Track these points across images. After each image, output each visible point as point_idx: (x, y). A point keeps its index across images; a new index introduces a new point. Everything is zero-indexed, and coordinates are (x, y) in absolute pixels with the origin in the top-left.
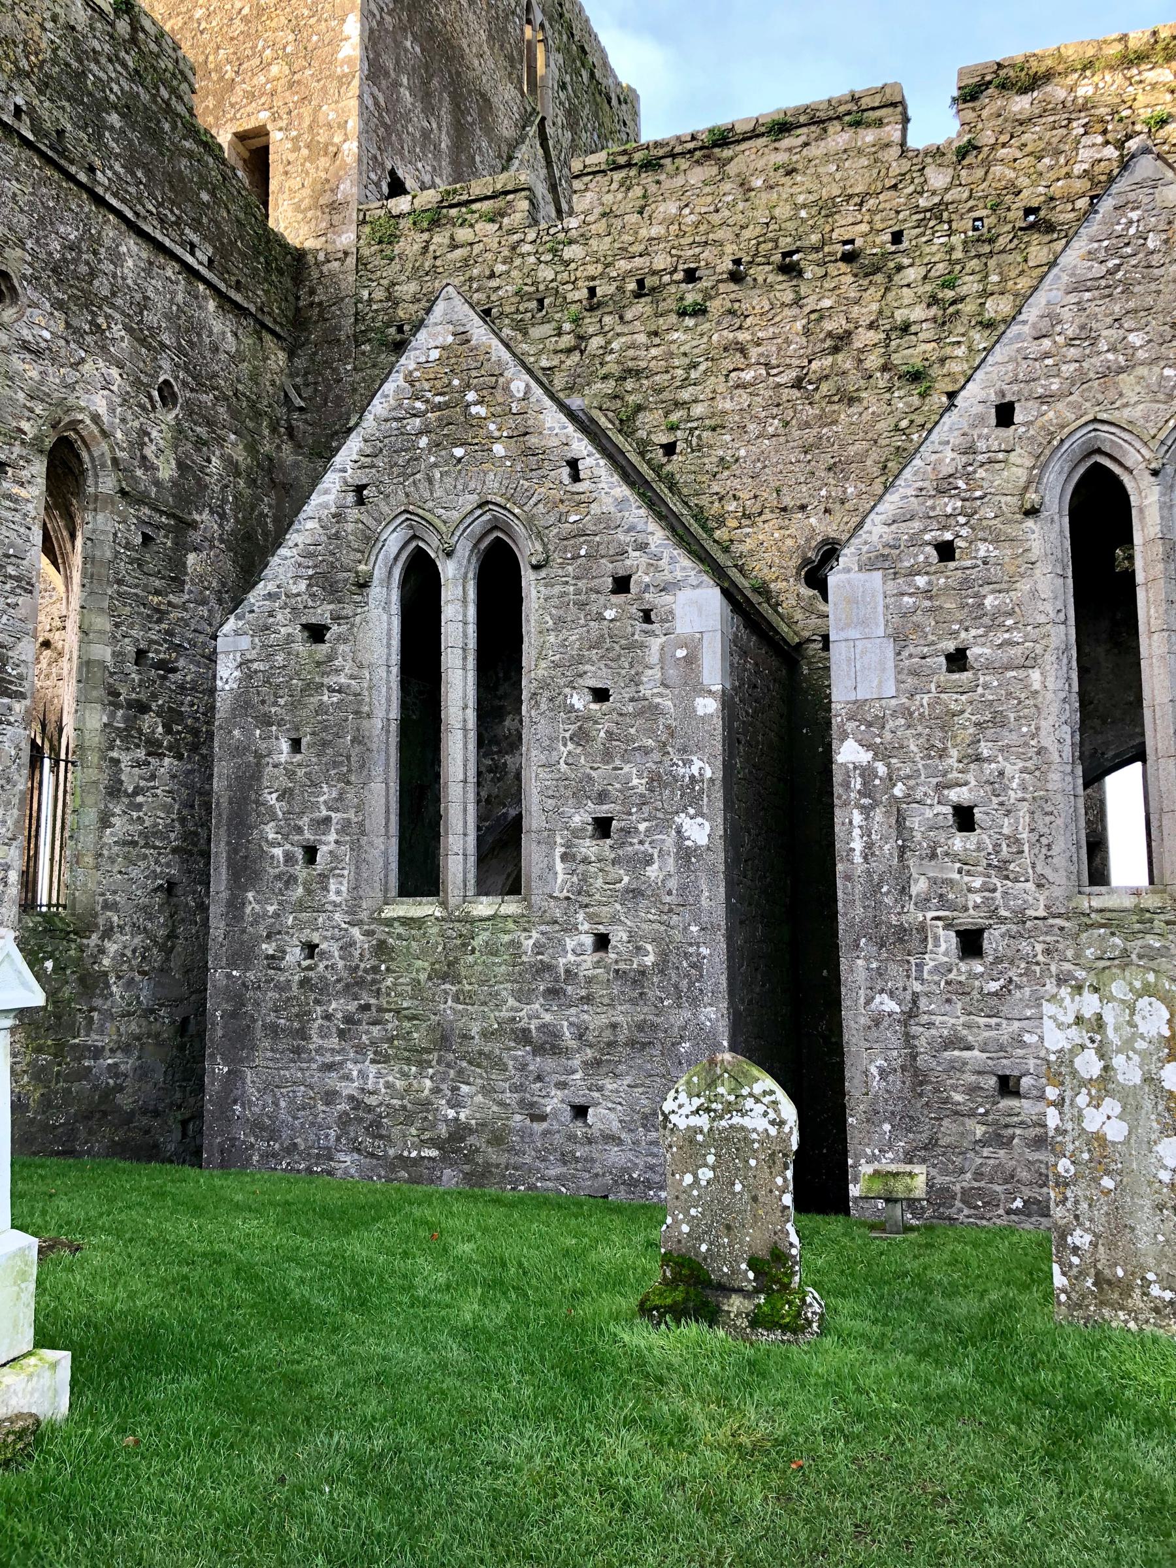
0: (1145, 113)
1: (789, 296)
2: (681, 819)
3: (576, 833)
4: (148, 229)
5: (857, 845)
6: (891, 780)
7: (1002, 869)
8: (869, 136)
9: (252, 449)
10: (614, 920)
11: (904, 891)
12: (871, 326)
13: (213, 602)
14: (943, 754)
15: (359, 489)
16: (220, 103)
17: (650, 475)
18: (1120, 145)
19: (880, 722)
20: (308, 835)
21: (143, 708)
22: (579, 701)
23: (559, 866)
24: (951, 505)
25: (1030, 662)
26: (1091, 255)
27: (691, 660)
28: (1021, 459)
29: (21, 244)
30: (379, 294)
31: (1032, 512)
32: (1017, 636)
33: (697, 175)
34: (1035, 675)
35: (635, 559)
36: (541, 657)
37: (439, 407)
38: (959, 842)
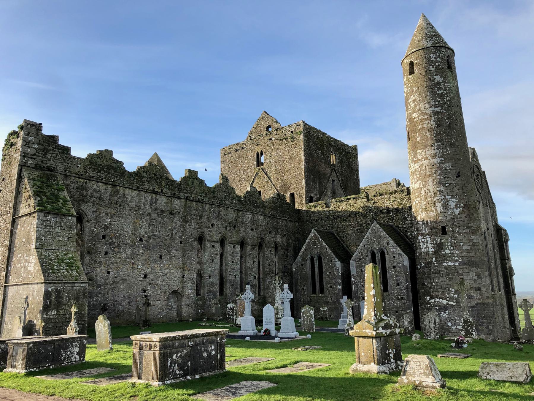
0: (392, 200)
1: (355, 219)
3: (329, 287)
6: (356, 282)
8: (363, 200)
9: (295, 237)
10: (332, 296)
11: (358, 293)
12: (364, 223)
13: (291, 258)
14: (361, 280)
15: (306, 250)
16: (288, 189)
17: (341, 241)
19: (355, 276)
20: (303, 287)
21: (285, 272)
24: (360, 255)
27: (338, 269)
28: (366, 251)
30: (309, 216)
31: (367, 256)
33: (345, 203)
36: (324, 268)
37: (313, 241)
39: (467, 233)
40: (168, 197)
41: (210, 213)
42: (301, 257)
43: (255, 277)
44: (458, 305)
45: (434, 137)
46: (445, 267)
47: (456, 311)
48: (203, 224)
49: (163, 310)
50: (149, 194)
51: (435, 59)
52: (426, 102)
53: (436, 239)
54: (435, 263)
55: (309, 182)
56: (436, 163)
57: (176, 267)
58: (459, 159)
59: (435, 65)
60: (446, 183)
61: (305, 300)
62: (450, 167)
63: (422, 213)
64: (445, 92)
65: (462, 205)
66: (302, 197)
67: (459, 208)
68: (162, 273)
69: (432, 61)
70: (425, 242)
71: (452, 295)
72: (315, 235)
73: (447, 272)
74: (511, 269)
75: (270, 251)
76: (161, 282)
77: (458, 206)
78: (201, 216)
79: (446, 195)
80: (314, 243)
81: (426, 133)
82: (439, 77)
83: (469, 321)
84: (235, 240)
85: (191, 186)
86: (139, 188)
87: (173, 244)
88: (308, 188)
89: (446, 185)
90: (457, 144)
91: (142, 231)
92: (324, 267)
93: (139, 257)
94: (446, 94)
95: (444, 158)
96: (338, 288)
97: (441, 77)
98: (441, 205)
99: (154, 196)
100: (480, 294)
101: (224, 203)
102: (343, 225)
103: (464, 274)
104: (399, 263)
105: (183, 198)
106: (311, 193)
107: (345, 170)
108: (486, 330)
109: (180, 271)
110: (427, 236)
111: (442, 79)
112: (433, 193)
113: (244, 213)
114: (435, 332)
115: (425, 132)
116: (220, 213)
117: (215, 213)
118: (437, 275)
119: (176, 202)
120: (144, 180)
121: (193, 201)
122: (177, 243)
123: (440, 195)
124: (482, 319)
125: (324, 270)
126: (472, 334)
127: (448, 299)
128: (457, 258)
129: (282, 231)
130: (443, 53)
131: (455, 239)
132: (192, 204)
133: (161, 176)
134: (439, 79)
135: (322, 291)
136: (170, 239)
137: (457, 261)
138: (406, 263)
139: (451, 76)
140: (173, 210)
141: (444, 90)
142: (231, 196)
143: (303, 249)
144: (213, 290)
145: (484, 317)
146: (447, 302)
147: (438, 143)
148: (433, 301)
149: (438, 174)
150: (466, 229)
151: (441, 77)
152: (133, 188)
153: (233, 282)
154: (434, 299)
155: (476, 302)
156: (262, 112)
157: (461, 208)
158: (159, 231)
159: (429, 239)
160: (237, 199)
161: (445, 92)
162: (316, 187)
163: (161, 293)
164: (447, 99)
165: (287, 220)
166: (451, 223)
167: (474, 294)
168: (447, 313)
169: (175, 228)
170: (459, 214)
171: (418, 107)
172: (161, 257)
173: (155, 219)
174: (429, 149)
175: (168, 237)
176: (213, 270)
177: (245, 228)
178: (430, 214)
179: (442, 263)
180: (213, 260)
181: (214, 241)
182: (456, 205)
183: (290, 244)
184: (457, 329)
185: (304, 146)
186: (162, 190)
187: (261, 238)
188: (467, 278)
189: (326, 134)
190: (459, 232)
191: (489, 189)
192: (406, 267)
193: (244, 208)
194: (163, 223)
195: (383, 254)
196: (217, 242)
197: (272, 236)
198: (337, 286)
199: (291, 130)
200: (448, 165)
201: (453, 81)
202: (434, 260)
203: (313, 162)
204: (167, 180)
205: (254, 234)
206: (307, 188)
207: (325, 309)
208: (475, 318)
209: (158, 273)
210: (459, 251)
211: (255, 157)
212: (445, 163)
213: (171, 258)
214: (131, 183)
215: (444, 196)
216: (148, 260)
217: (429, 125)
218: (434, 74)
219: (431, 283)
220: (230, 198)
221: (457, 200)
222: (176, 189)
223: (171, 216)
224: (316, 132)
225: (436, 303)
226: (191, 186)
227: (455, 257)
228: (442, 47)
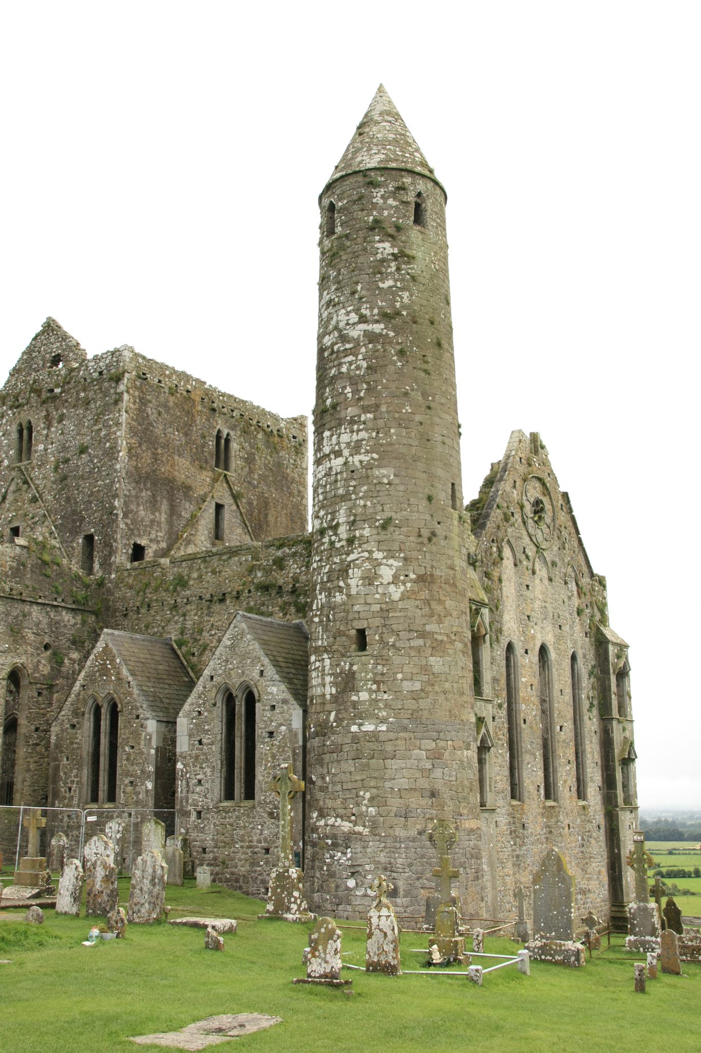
2: (147, 782)
3: (126, 786)
5: (179, 790)
7: (205, 796)
11: (187, 802)
15: (84, 686)
18: (300, 568)
20: (69, 785)
22: (127, 749)
23: (122, 795)
25: (212, 743)
26: (228, 639)
27: (150, 739)
28: (214, 691)
32: (210, 737)
34: (214, 747)
35: (141, 711)
37: (101, 664)
38: (198, 789)
39: (419, 650)
42: (72, 705)
44: (376, 835)
46: (355, 739)
47: (369, 850)
51: (381, 201)
52: (352, 308)
53: (342, 663)
54: (335, 724)
55: (133, 507)
56: (357, 464)
60: (378, 518)
61: (73, 818)
62: (392, 477)
63: (320, 594)
65: (412, 576)
67: (404, 583)
70: (320, 669)
71: (364, 808)
72: (106, 648)
73: (357, 750)
74: (629, 744)
77: (402, 578)
79: (374, 549)
80: (104, 671)
81: (345, 387)
82: (387, 245)
83: (286, 874)
88: (129, 522)
89: (377, 524)
92: (123, 733)
96: (146, 787)
98: (360, 575)
102: (194, 624)
104: (281, 725)
106: (139, 536)
107: (263, 478)
110: (325, 656)
112: (344, 543)
114: (150, 903)
115: (343, 385)
118: (335, 755)
123: (360, 550)
125: (119, 741)
126: (289, 910)
127: (353, 818)
131: (384, 662)
134: (387, 251)
135: (112, 797)
137: (383, 721)
138: (297, 724)
141: (396, 281)
143: (78, 684)
146: (351, 825)
147: (369, 415)
148: (322, 823)
149: (361, 494)
150: (418, 637)
154: (324, 817)
155: (419, 827)
159: (327, 662)
161: (399, 284)
162: (159, 523)
164: (402, 302)
166: (377, 622)
168: (349, 855)
170: (401, 599)
171: (333, 322)
174: (348, 430)
178: (335, 597)
179: (348, 726)
182: (396, 577)
183: (59, 671)
184: (366, 895)
188: (403, 765)
189: (205, 383)
192: (296, 734)
195: (251, 700)
198: (143, 784)
199: (99, 370)
202: (332, 717)
203: (153, 454)
206: (127, 524)
207: (62, 843)
211: (15, 435)
212: (379, 467)
215: (371, 552)
217: (353, 367)
218: (377, 238)
219: (323, 778)
221: (401, 564)
224: (169, 377)
225: (328, 828)
227: (379, 709)
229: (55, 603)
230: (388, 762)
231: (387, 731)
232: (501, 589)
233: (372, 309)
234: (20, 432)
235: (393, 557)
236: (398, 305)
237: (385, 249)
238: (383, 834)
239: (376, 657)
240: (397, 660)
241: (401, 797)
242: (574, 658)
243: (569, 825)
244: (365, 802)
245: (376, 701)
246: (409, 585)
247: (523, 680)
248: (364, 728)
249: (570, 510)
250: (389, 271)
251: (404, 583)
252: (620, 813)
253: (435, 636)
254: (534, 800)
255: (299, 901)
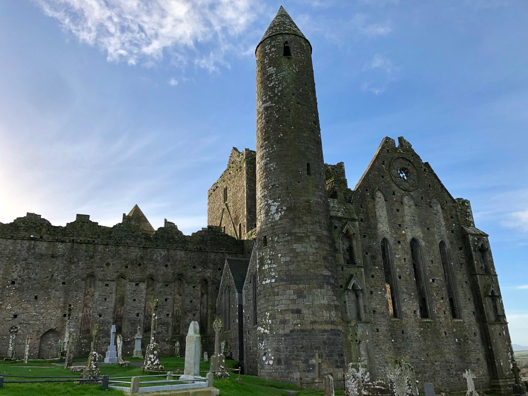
4: (215, 251)
29: (197, 262)
39: (288, 241)
40: (50, 242)
41: (104, 253)
43: (168, 315)
45: (263, 136)
47: (269, 341)
48: (94, 264)
49: (35, 348)
50: (27, 241)
51: (269, 51)
56: (263, 164)
57: (55, 307)
58: (286, 156)
59: (269, 56)
60: (270, 185)
64: (277, 83)
65: (284, 208)
66: (244, 226)
67: (281, 212)
68: (37, 312)
69: (267, 54)
71: (267, 320)
75: (194, 287)
76: (34, 322)
78: (92, 257)
82: (272, 67)
84: (138, 278)
85: (80, 229)
86: (13, 237)
87: (53, 285)
88: (252, 216)
89: (269, 188)
90: (285, 138)
91: (15, 275)
93: (9, 299)
94: (279, 84)
95: (269, 157)
97: (273, 68)
99: (33, 242)
100: (299, 318)
101: (124, 242)
103: (280, 293)
105: (68, 241)
108: (302, 366)
109: (60, 310)
111: (275, 69)
113: (153, 251)
116: (118, 252)
117: (112, 253)
119: (60, 246)
120: (20, 230)
121: (81, 243)
122: (59, 284)
124: (298, 351)
128: (274, 274)
129: (215, 264)
130: (279, 41)
132: (81, 246)
133: (42, 224)
134: (271, 71)
136: (50, 280)
137: (274, 277)
139: (286, 63)
140: (56, 254)
141: (275, 82)
142: (134, 234)
144: (104, 328)
145: (301, 348)
151: (273, 68)
152: (7, 237)
153: (134, 321)
155: (291, 329)
156: (232, 148)
157: (283, 212)
158: (36, 274)
160: (143, 236)
163: (34, 331)
164: (278, 90)
165: (223, 253)
166: (269, 232)
167: (289, 318)
169: (57, 270)
170: (280, 219)
172: (36, 298)
173: (31, 263)
175: (47, 279)
176: (105, 308)
177: (155, 265)
180: (106, 299)
181: (108, 280)
182: (277, 210)
184: (269, 364)
185: (247, 173)
186: (41, 237)
187: (179, 274)
188: (282, 298)
190: (279, 241)
191: (442, 186)
193: (153, 245)
194: (41, 266)
196: (112, 281)
197: (198, 271)
200: (272, 165)
201: (289, 68)
204: (49, 226)
205: (170, 270)
206: (250, 217)
208: (288, 349)
209: (31, 313)
210: (276, 264)
212: (269, 163)
213: (49, 299)
214: (4, 234)
215: (267, 201)
216: (20, 302)
220: (132, 236)
221: (279, 204)
222: (59, 234)
223: (52, 259)
226: (80, 229)
228: (277, 35)
229: (222, 251)
230: (276, 297)
231: (275, 282)
232: (375, 212)
233: (266, 97)
234: (224, 191)
235: (276, 201)
236: (276, 91)
237: (270, 70)
238: (275, 333)
239: (270, 248)
240: (278, 248)
241: (281, 314)
242: (442, 244)
243: (445, 333)
244: (268, 318)
245: (271, 268)
246: (283, 212)
247: (397, 256)
248: (267, 282)
249: (432, 171)
250: (272, 79)
251: (281, 212)
252: (489, 327)
253: (297, 234)
254: (411, 318)
255: (153, 360)
